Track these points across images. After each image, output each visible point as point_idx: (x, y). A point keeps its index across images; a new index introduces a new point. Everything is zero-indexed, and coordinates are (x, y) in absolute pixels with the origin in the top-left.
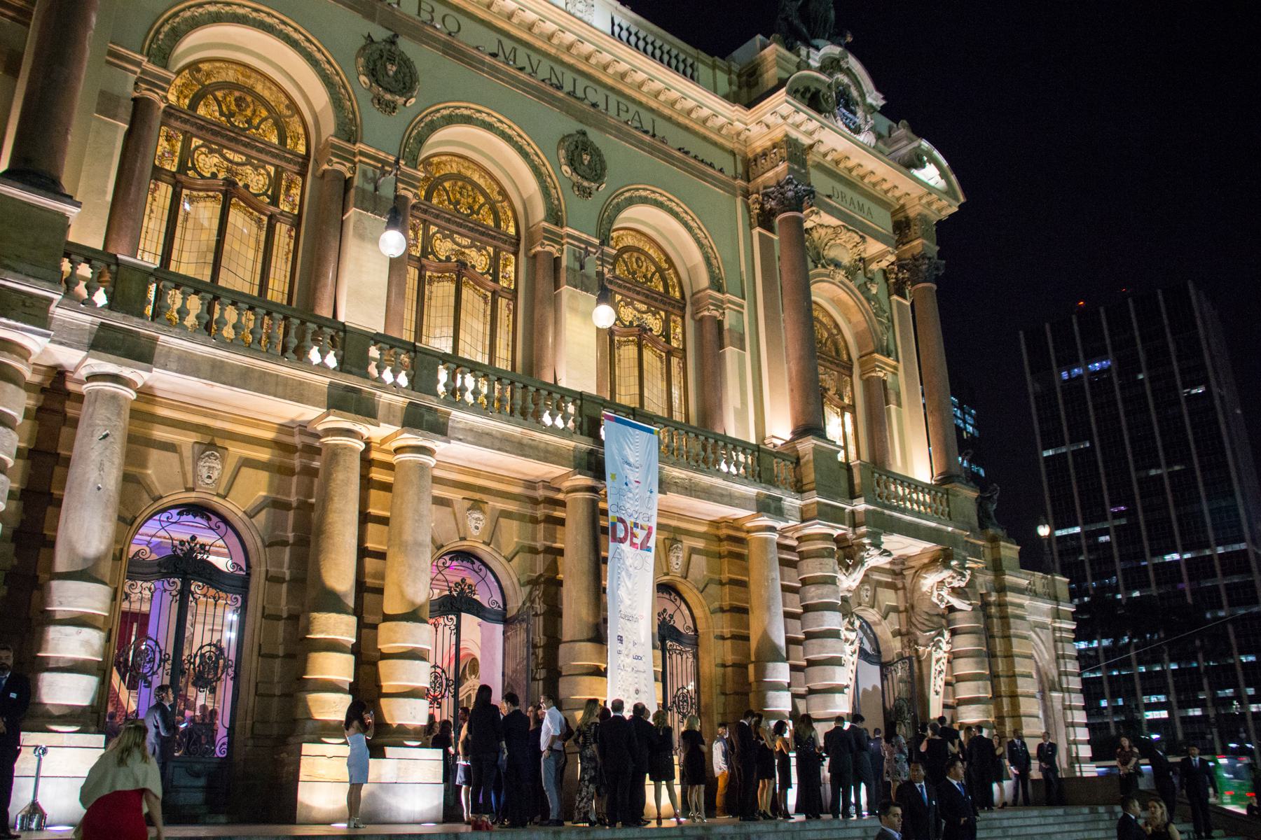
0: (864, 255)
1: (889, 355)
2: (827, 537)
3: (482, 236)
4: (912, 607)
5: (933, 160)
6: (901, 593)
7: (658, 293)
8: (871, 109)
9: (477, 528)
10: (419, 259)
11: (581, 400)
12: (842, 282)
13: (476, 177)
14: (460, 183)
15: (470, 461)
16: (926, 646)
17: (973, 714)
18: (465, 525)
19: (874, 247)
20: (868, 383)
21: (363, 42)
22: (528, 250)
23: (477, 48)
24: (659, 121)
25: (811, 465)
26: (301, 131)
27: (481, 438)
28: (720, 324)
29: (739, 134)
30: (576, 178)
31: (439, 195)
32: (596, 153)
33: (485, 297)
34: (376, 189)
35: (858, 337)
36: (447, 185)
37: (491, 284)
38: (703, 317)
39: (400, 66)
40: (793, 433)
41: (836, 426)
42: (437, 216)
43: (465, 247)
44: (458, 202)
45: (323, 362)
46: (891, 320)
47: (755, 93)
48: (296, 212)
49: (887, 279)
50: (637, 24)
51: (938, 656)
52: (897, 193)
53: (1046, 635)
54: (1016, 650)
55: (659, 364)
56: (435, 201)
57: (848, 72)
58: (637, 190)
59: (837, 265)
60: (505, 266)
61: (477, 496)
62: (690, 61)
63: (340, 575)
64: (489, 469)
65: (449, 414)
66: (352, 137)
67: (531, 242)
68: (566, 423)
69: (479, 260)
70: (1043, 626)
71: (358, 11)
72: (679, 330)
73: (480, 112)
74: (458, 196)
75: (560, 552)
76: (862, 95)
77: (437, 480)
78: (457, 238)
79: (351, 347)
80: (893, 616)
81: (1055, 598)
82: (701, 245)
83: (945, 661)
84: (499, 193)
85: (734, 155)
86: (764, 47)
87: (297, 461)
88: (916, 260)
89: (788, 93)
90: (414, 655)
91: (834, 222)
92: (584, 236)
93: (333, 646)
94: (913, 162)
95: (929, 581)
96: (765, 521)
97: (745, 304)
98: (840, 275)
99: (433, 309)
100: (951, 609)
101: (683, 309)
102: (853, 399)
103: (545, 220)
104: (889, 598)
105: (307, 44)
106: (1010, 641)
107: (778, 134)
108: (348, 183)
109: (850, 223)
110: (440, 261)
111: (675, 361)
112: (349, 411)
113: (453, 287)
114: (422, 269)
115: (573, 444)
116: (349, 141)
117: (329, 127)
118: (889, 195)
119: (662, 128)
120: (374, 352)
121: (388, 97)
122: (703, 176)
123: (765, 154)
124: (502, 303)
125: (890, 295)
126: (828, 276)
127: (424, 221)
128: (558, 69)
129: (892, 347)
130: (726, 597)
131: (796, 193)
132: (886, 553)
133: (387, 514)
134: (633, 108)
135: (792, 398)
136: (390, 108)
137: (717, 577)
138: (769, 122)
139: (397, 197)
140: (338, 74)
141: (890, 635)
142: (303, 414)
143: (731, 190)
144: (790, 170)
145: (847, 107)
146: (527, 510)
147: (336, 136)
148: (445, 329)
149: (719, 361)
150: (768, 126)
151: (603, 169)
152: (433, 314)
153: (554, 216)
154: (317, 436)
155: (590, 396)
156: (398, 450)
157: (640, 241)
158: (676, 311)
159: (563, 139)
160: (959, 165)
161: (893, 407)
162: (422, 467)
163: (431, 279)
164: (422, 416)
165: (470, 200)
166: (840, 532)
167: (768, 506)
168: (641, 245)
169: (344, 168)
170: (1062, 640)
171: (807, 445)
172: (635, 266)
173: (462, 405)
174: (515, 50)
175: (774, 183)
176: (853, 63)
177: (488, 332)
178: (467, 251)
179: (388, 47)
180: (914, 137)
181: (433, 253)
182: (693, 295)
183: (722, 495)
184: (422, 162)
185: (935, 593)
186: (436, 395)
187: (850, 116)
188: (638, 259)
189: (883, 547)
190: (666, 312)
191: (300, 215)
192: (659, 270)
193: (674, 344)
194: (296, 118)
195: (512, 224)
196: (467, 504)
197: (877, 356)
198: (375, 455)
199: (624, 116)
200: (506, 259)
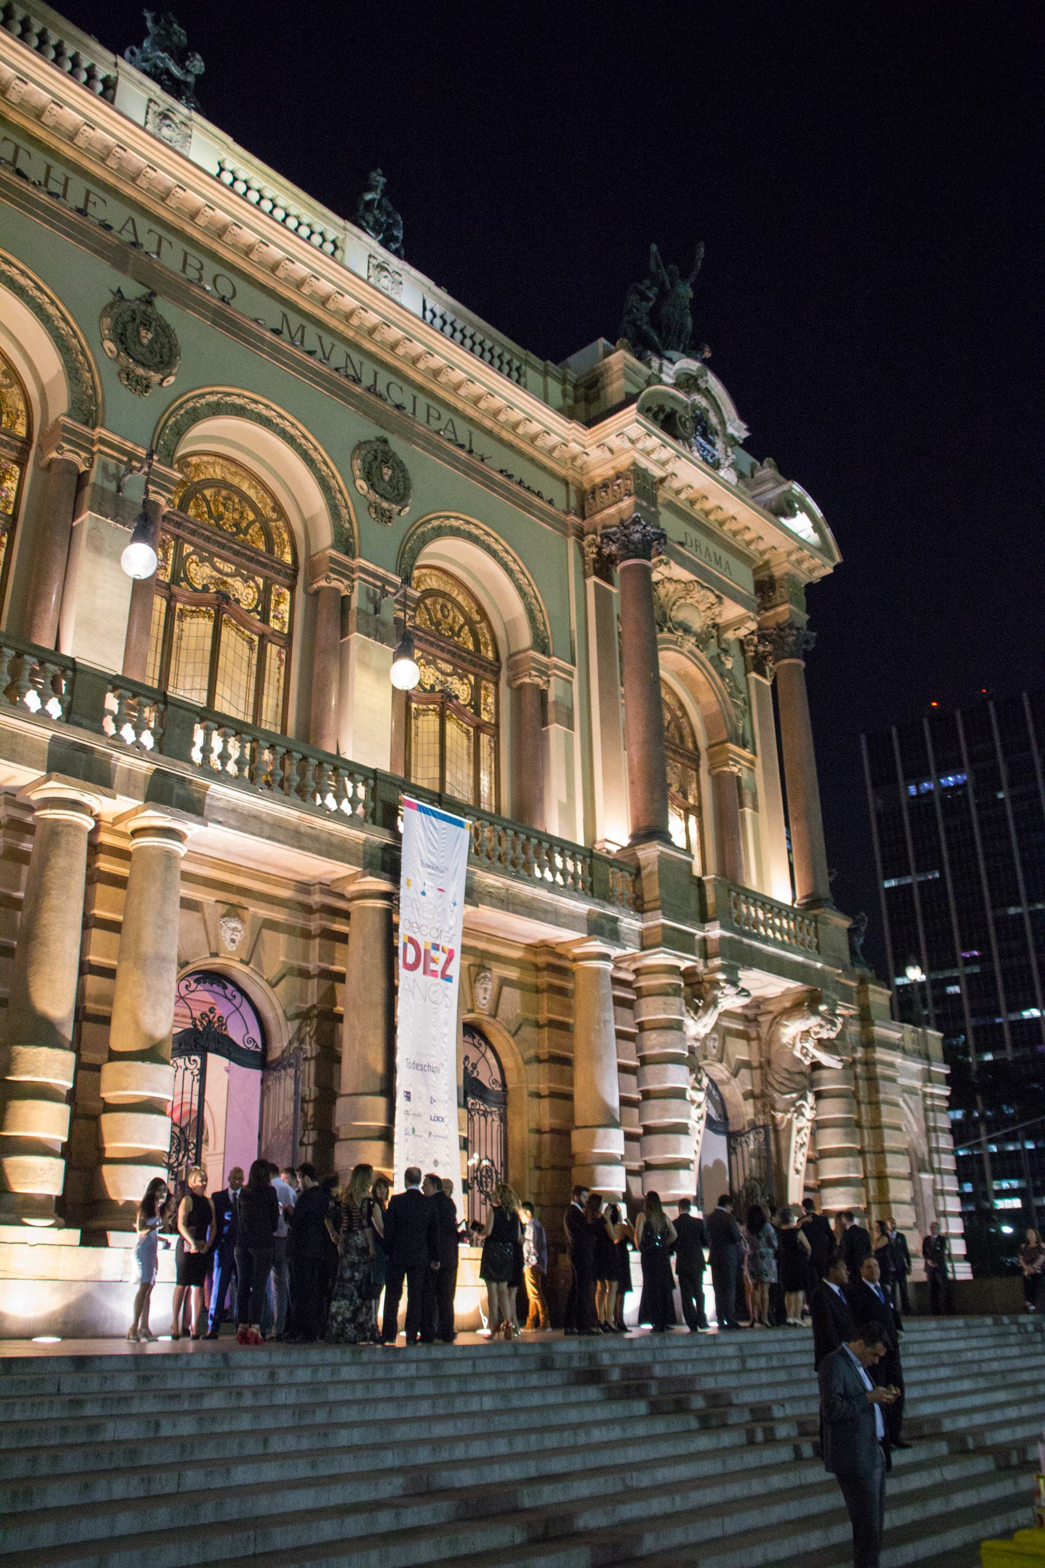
0: (719, 620)
1: (744, 746)
2: (673, 970)
3: (250, 561)
4: (769, 1062)
6: (754, 1044)
7: (468, 652)
8: (731, 441)
9: (233, 941)
10: (168, 587)
11: (375, 779)
12: (691, 652)
13: (245, 487)
14: (224, 493)
15: (228, 853)
16: (786, 1111)
17: (841, 1198)
18: (217, 936)
19: (732, 611)
20: (718, 780)
21: (109, 298)
22: (307, 584)
23: (256, 321)
24: (476, 433)
25: (656, 877)
26: (21, 406)
27: (247, 822)
28: (543, 694)
29: (574, 458)
30: (373, 497)
31: (197, 506)
32: (399, 467)
33: (250, 642)
34: (119, 489)
35: (706, 720)
36: (208, 493)
37: (259, 624)
38: (523, 684)
39: (157, 335)
40: (633, 836)
41: (679, 828)
42: (193, 533)
43: (227, 575)
44: (221, 517)
45: (43, 709)
46: (747, 702)
47: (595, 410)
48: (10, 512)
49: (744, 652)
50: (454, 311)
51: (800, 1122)
52: (762, 546)
53: (915, 1102)
54: (885, 1119)
55: (465, 741)
56: (192, 512)
57: (707, 393)
58: (448, 518)
59: (687, 630)
60: (278, 603)
61: (235, 899)
62: (516, 363)
63: (55, 996)
64: (252, 865)
65: (207, 788)
66: (90, 420)
67: (312, 575)
68: (354, 808)
69: (245, 593)
70: (911, 1091)
71: (107, 259)
72: (490, 700)
73: (256, 402)
74: (221, 509)
75: (341, 977)
76: (723, 423)
77: (186, 876)
78: (219, 564)
79: (82, 691)
80: (744, 1072)
81: (927, 1057)
83: (807, 1131)
84: (274, 509)
85: (567, 484)
86: (608, 353)
88: (781, 630)
89: (640, 410)
90: (150, 1107)
91: (685, 575)
92: (381, 571)
93: (43, 1093)
94: (783, 509)
95: (791, 1030)
96: (597, 946)
97: (576, 671)
98: (690, 643)
99: (183, 653)
100: (816, 1066)
101: (497, 673)
102: (699, 798)
103: (333, 547)
104: (740, 1050)
105: (38, 293)
106: (878, 1109)
107: (623, 462)
108: (81, 479)
109: (706, 578)
110: (196, 590)
111: (485, 738)
112: (76, 776)
113: (210, 624)
114: (171, 599)
115: (363, 836)
116: (86, 423)
117: (60, 404)
118: (752, 547)
119: (482, 444)
120: (111, 702)
121: (140, 371)
122: (528, 507)
123: (605, 485)
124: (272, 650)
125: (747, 672)
126: (675, 643)
127: (177, 538)
128: (356, 357)
129: (748, 736)
130: (546, 1043)
131: (644, 536)
132: (744, 992)
133: (120, 918)
134: (446, 415)
135: (633, 793)
136: (142, 386)
137: (531, 1016)
138: (613, 446)
139: (146, 502)
140: (76, 336)
141: (741, 1098)
142: (12, 777)
143: (562, 528)
144: (638, 507)
145: (704, 435)
146: (298, 921)
147: (69, 415)
148: (198, 680)
149: (541, 741)
150: (611, 450)
151: (408, 488)
152: (182, 659)
153: (344, 542)
154: (30, 809)
155: (385, 775)
156: (136, 833)
157: (446, 583)
158: (489, 676)
159: (360, 446)
160: (837, 517)
161: (748, 811)
162: (169, 856)
163: (183, 614)
164: (171, 789)
165: (237, 516)
166: (689, 964)
167: (603, 928)
168: (447, 589)
169: (79, 459)
170: (933, 1108)
171: (650, 853)
172: (439, 615)
173: (220, 776)
174: (303, 328)
175: (616, 521)
176: (713, 383)
177: (253, 687)
178: (230, 580)
179: (143, 307)
180: (782, 479)
181: (186, 579)
182: (511, 656)
183: (546, 912)
184: (178, 461)
185: (798, 1046)
186: (191, 762)
187: (708, 447)
188: (443, 606)
189: (741, 984)
190: (476, 676)
191: (14, 517)
192: (469, 622)
193: (485, 717)
194: (16, 390)
195: (288, 550)
196: (222, 909)
197: (731, 746)
198: (104, 838)
199: (435, 425)
200: (279, 595)
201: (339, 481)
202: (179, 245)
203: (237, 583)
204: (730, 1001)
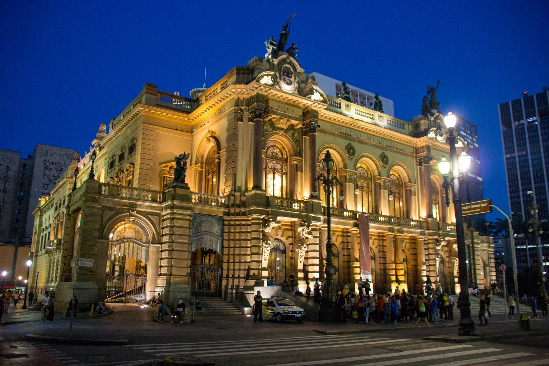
2: (433, 239)
5: (460, 140)
28: (410, 190)
53: (486, 253)
54: (476, 258)
70: (485, 250)
75: (385, 246)
81: (489, 243)
82: (407, 172)
86: (421, 119)
87: (345, 234)
93: (357, 267)
104: (446, 249)
119: (399, 146)
143: (412, 157)
153: (380, 174)
170: (490, 254)
171: (430, 220)
201: (378, 163)
202: (353, 131)
203: (364, 184)
204: (443, 243)
